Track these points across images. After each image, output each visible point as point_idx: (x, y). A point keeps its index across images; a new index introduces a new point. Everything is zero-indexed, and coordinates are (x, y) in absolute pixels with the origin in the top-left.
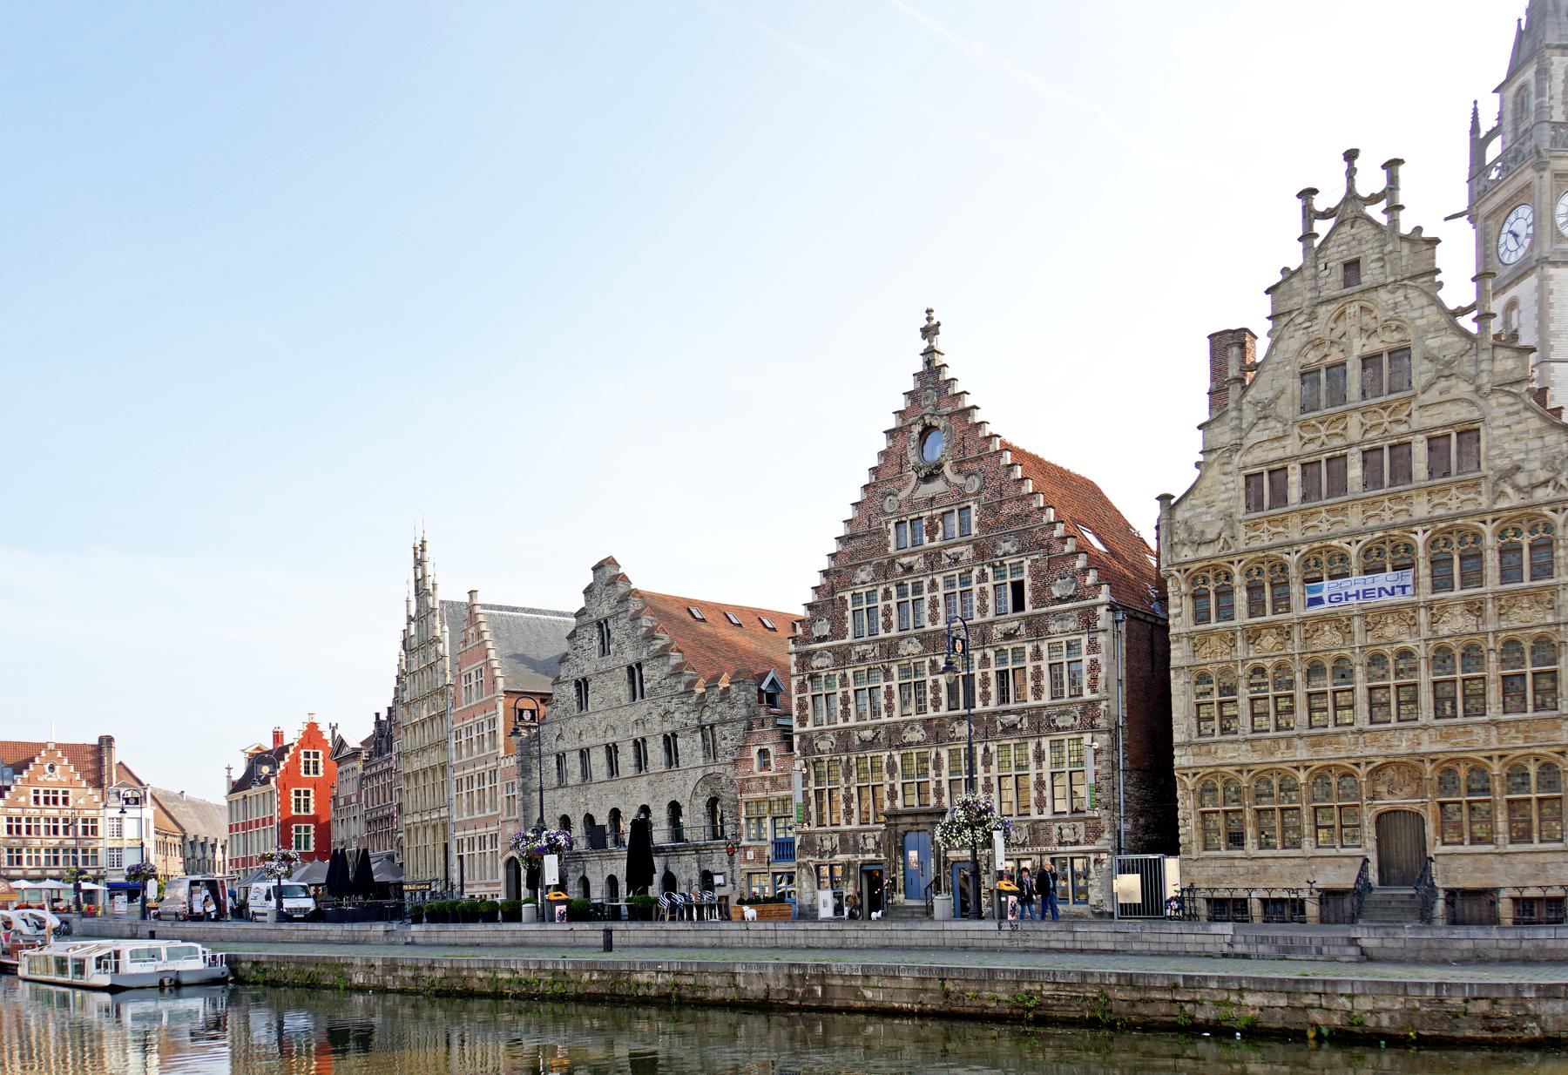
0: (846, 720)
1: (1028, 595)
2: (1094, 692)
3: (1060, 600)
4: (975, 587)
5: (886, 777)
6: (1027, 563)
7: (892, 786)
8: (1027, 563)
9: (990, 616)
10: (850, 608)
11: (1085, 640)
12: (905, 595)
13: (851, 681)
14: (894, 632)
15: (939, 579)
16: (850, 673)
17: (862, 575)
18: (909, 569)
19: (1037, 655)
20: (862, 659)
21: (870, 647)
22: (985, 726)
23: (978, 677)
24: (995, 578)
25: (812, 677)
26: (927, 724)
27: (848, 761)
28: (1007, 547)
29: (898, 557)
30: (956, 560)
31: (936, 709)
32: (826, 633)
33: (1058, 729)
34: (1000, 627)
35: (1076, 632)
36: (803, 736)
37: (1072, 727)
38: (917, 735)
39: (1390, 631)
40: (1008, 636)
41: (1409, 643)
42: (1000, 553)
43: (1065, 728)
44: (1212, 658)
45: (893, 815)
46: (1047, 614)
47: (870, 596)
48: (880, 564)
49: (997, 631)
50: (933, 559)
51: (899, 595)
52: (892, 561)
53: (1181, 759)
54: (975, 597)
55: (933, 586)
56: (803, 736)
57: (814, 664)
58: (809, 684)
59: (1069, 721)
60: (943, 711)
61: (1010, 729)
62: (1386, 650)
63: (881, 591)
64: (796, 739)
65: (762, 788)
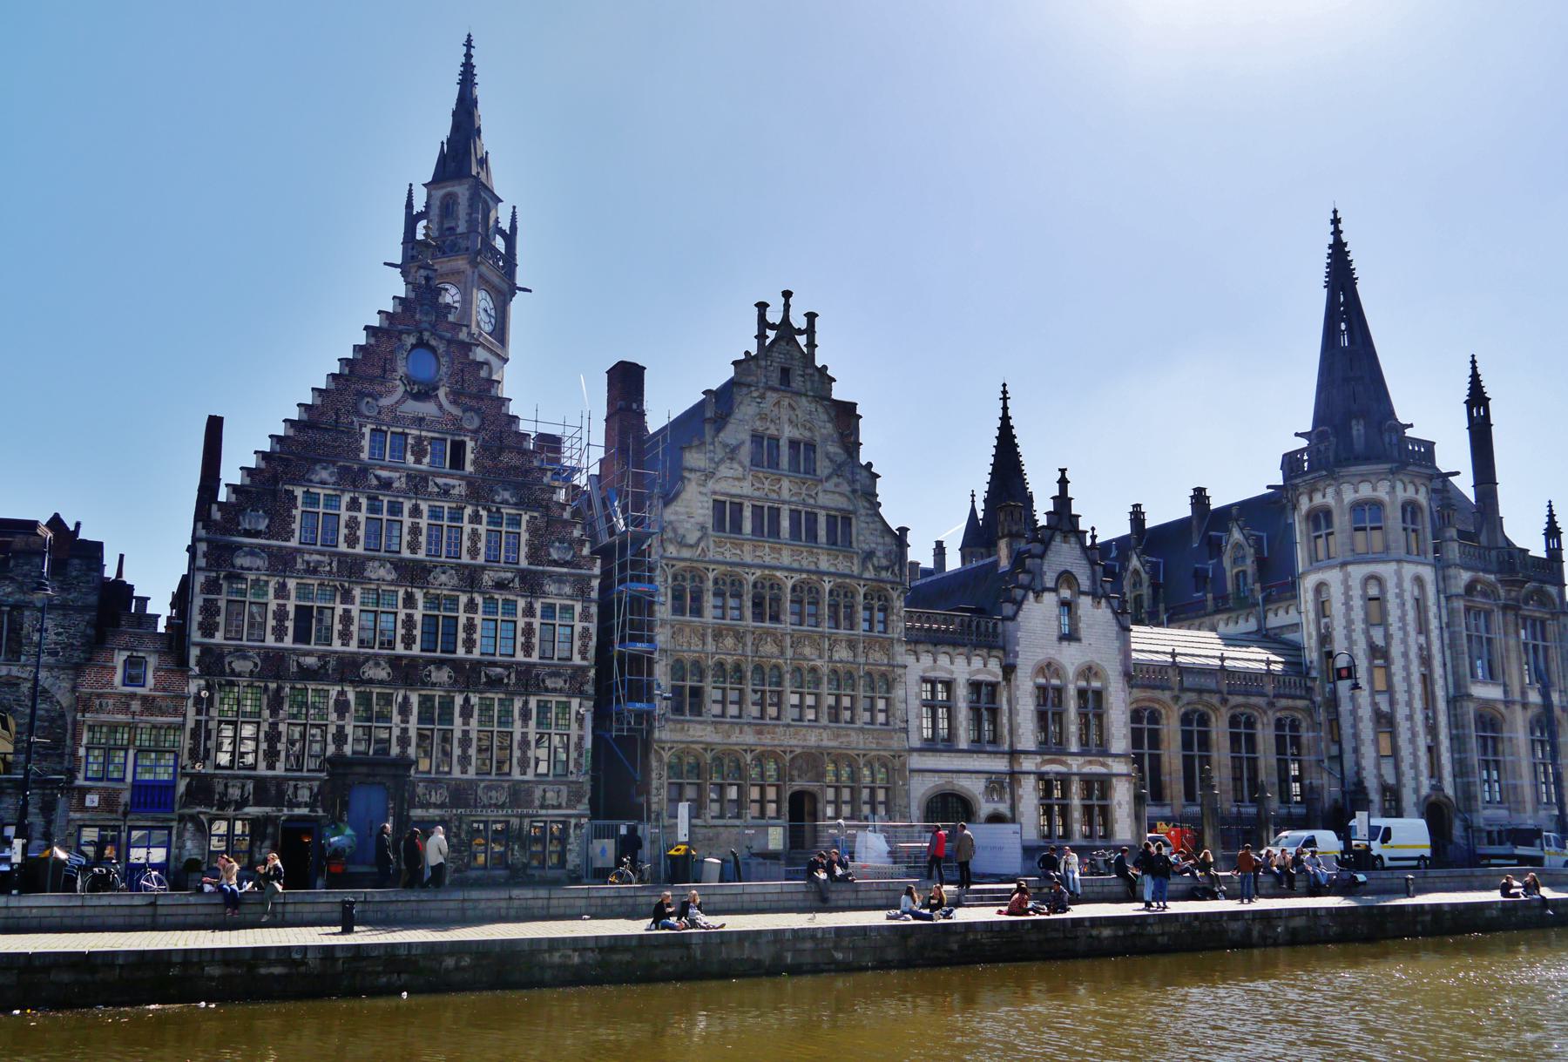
0: (280, 639)
2: (584, 658)
3: (556, 563)
4: (467, 527)
5: (333, 716)
6: (525, 518)
8: (525, 518)
9: (481, 560)
10: (300, 509)
11: (578, 608)
12: (378, 510)
13: (293, 594)
14: (359, 549)
15: (424, 506)
17: (324, 475)
18: (386, 485)
19: (529, 611)
20: (312, 570)
21: (326, 559)
22: (468, 675)
23: (462, 620)
24: (489, 523)
26: (395, 661)
29: (373, 466)
31: (408, 646)
32: (262, 527)
33: (547, 690)
35: (571, 597)
36: (206, 650)
37: (561, 691)
38: (382, 673)
39: (807, 651)
40: (501, 585)
41: (819, 663)
42: (498, 499)
43: (555, 690)
44: (691, 648)
45: (337, 765)
46: (543, 573)
47: (332, 501)
48: (348, 469)
49: (487, 578)
51: (371, 509)
52: (364, 470)
53: (664, 734)
54: (465, 537)
55: (416, 512)
56: (206, 650)
57: (239, 561)
59: (560, 683)
60: (416, 650)
61: (495, 683)
62: (805, 664)
63: (346, 498)
64: (195, 652)
65: (126, 709)
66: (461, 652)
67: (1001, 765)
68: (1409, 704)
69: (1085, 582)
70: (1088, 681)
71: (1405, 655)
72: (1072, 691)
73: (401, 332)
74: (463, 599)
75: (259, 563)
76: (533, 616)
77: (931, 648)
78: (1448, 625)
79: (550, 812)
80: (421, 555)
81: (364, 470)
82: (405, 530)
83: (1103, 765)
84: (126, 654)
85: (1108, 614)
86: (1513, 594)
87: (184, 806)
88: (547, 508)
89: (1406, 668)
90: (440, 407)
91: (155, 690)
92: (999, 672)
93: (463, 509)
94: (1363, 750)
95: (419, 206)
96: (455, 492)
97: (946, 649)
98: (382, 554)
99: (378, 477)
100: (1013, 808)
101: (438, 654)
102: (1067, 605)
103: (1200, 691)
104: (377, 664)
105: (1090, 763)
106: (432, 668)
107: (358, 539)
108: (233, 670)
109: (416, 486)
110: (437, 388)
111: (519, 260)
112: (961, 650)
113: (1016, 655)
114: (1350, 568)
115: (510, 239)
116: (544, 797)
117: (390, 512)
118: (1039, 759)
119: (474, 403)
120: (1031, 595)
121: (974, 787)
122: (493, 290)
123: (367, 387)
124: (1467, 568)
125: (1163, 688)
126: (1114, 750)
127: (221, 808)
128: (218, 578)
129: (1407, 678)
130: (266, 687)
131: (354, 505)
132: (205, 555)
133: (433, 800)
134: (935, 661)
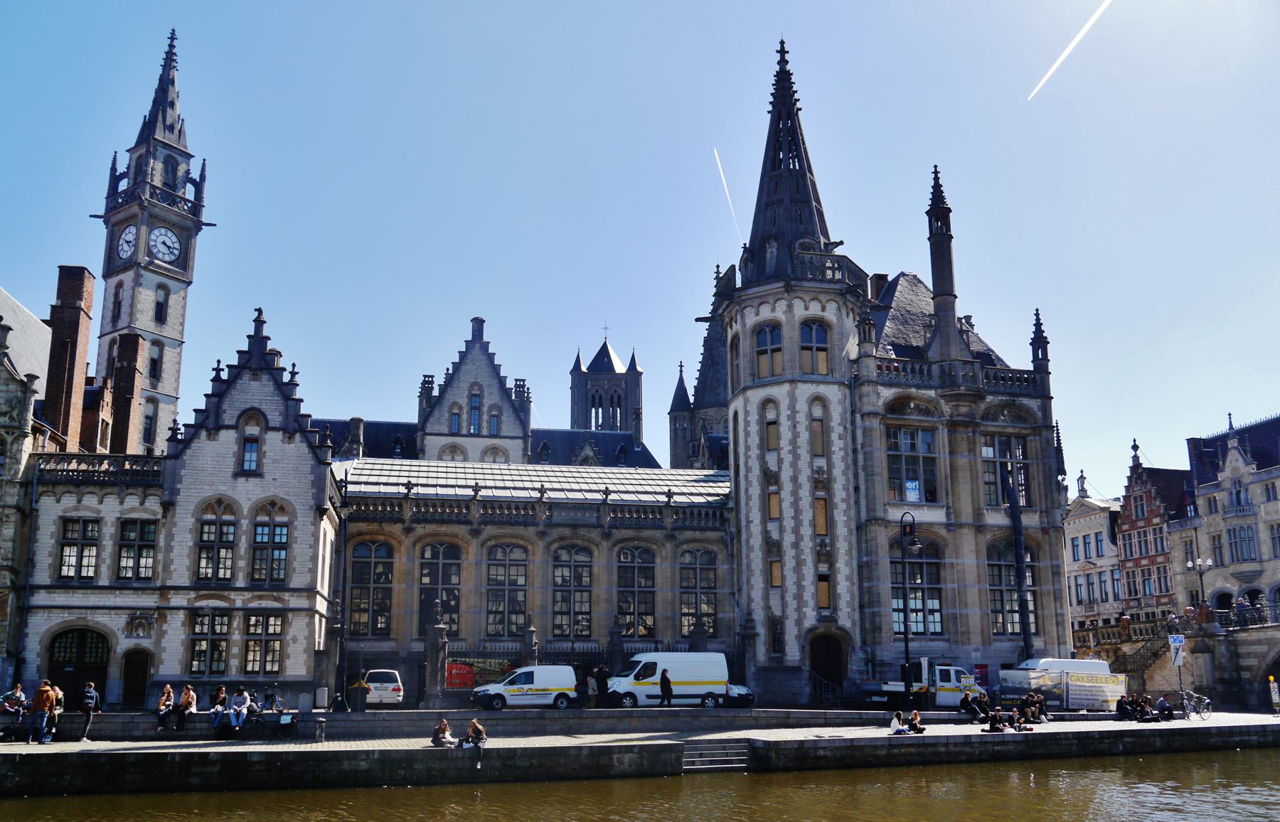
67: (149, 600)
68: (796, 531)
69: (275, 418)
70: (269, 515)
71: (794, 479)
72: (245, 523)
77: (72, 489)
78: (863, 446)
83: (277, 599)
85: (304, 448)
86: (964, 410)
89: (795, 493)
92: (159, 510)
94: (753, 581)
95: (121, 168)
97: (91, 489)
100: (158, 643)
102: (248, 442)
103: (574, 526)
105: (260, 598)
111: (206, 202)
112: (109, 490)
113: (177, 492)
114: (749, 393)
115: (199, 186)
118: (192, 595)
120: (204, 434)
121: (114, 623)
122: (170, 226)
124: (889, 385)
125: (526, 525)
126: (292, 585)
129: (795, 504)
134: (79, 501)
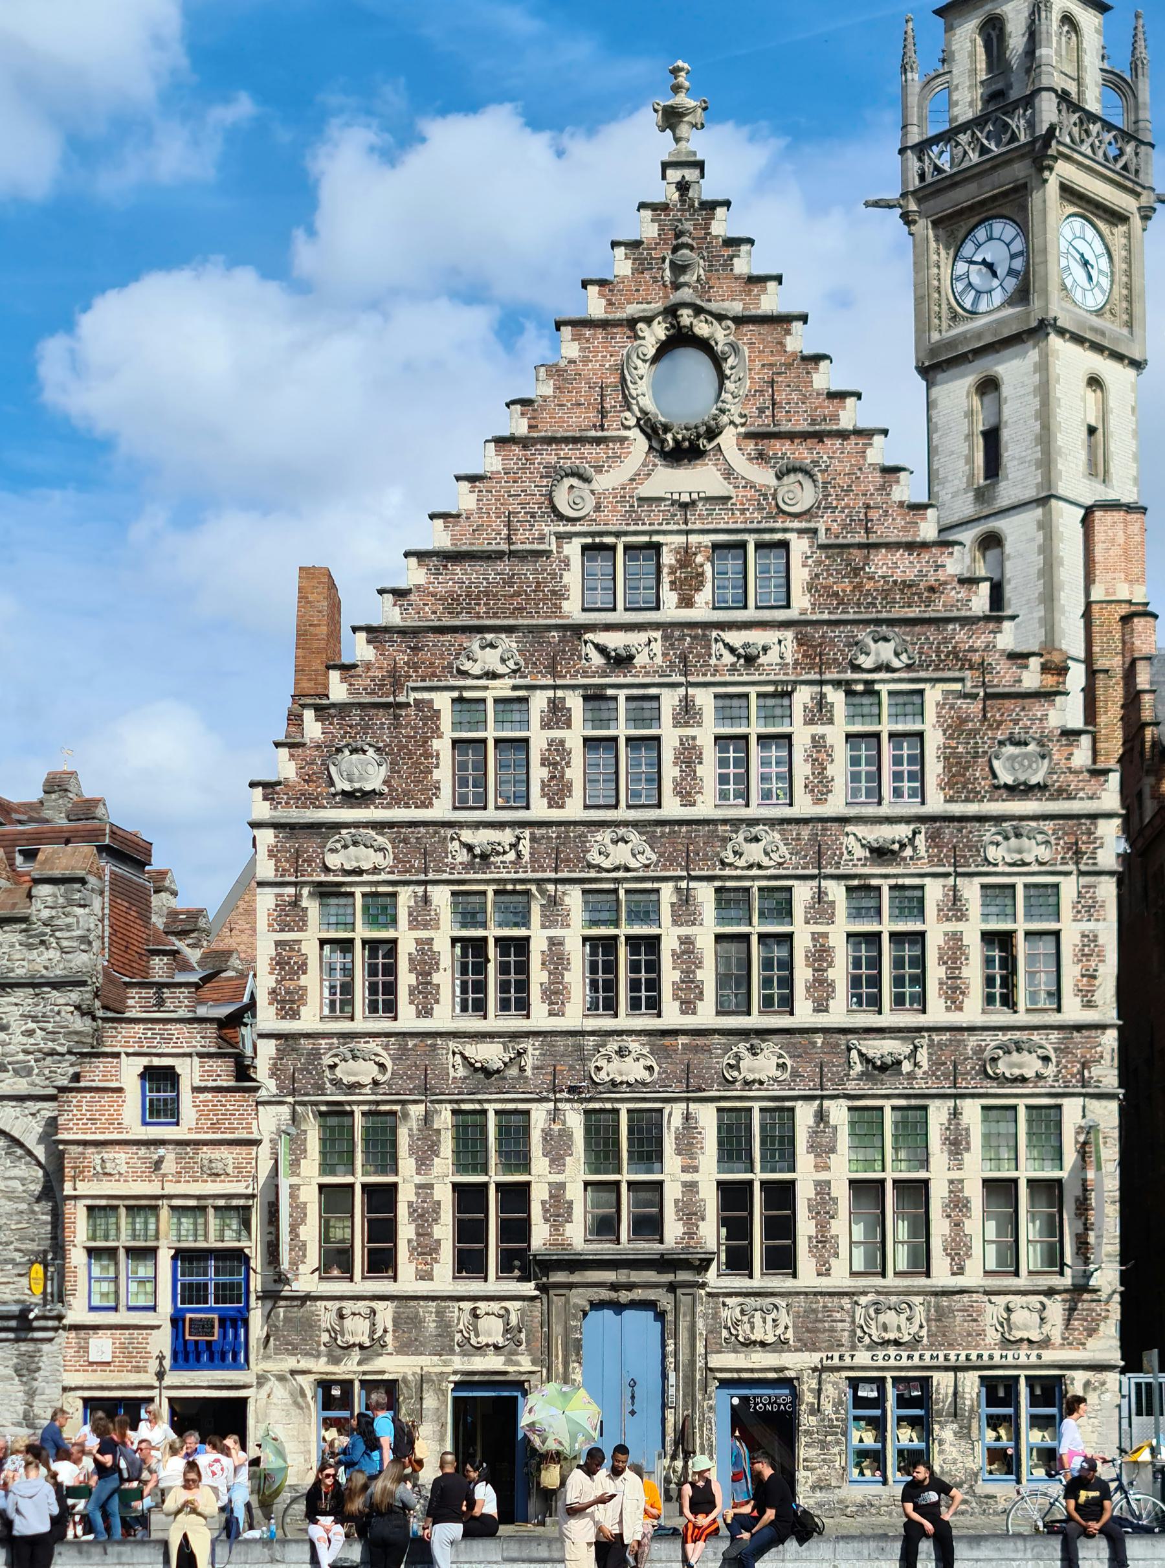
0: (425, 1012)
1: (934, 769)
4: (802, 735)
7: (558, 1190)
9: (836, 805)
10: (448, 732)
14: (574, 810)
15: (704, 699)
16: (441, 896)
18: (621, 661)
21: (506, 837)
23: (802, 942)
24: (851, 718)
25: (326, 892)
27: (427, 1119)
28: (885, 652)
30: (750, 660)
31: (687, 1006)
34: (861, 830)
42: (867, 662)
46: (981, 819)
49: (853, 844)
50: (688, 642)
55: (687, 712)
58: (312, 906)
63: (539, 702)
66: (804, 1014)
73: (632, 323)
74: (802, 893)
75: (377, 859)
76: (961, 916)
79: (1024, 1355)
80: (705, 807)
81: (578, 630)
82: (668, 756)
84: (145, 1061)
87: (267, 1357)
88: (983, 668)
90: (729, 473)
91: (198, 1130)
93: (789, 694)
96: (772, 657)
98: (622, 814)
99: (602, 650)
101: (755, 1020)
104: (621, 1052)
106: (742, 1048)
107: (568, 786)
108: (337, 1083)
109: (684, 658)
110: (712, 433)
116: (1006, 1323)
117: (635, 720)
119: (801, 453)
123: (570, 456)
127: (335, 1360)
128: (298, 897)
130: (406, 1116)
131: (557, 715)
132: (271, 854)
133: (757, 1336)
